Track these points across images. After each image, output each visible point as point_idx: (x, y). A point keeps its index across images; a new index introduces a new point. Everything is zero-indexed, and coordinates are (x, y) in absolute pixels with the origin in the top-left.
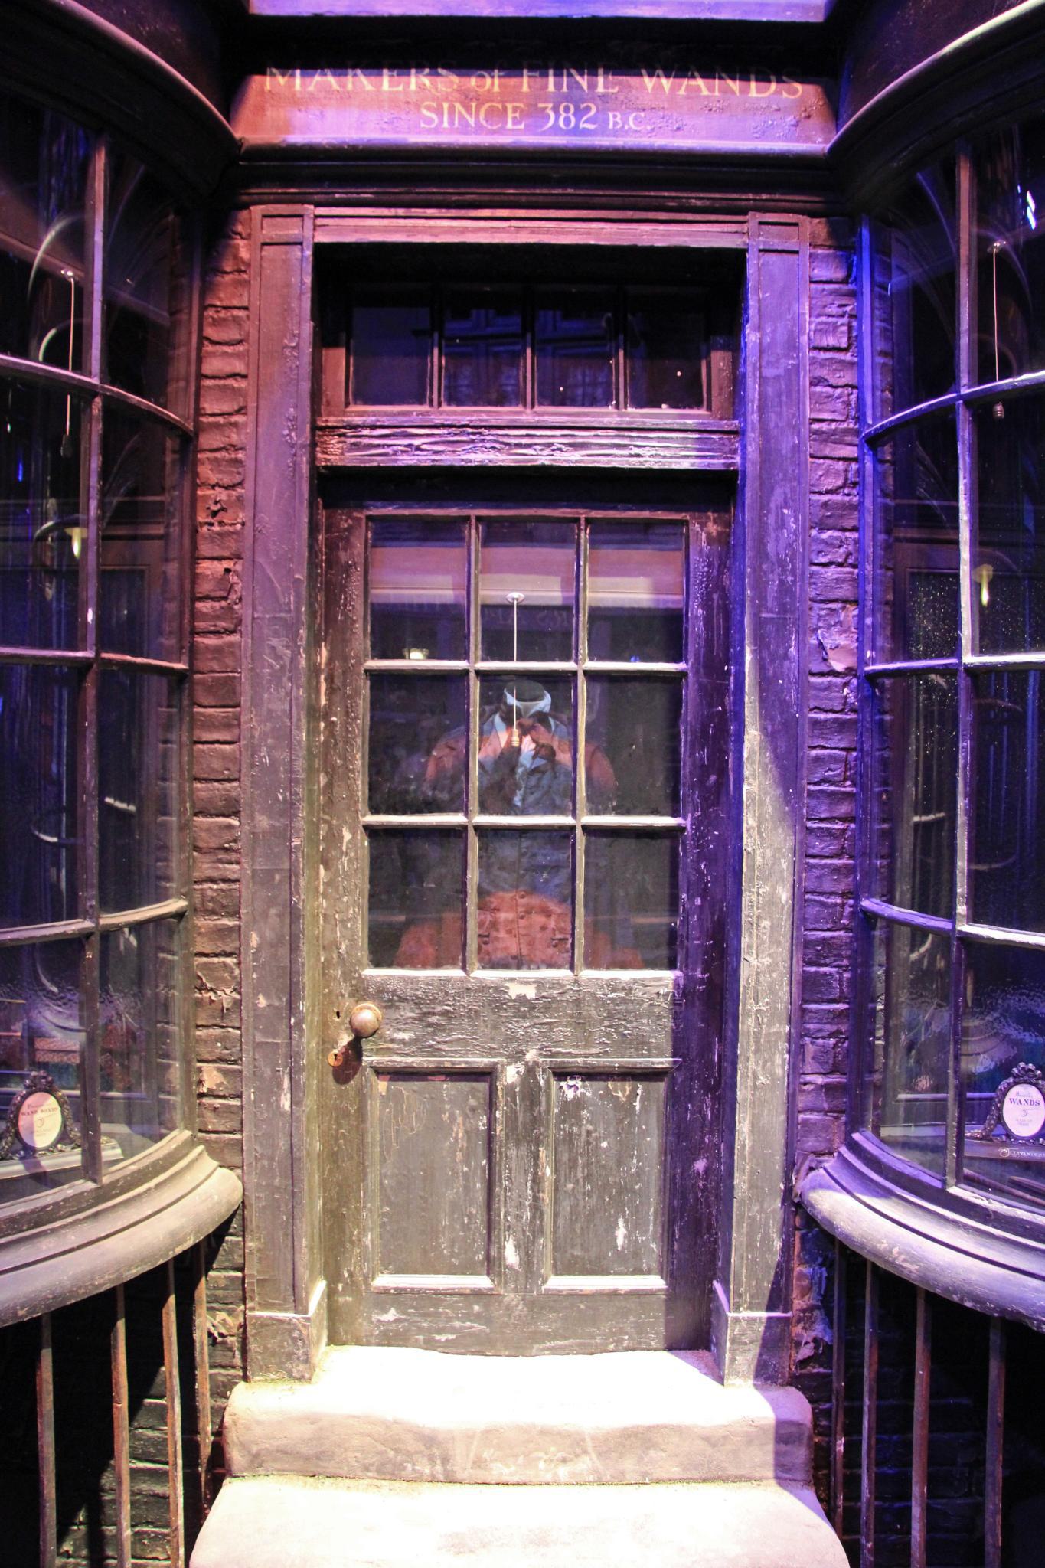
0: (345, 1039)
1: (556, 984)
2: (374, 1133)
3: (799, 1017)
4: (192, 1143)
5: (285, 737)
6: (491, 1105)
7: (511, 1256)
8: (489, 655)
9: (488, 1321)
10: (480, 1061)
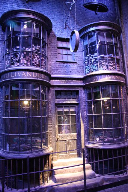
0: (57, 139)
3: (85, 135)
6: (66, 142)
10: (65, 140)
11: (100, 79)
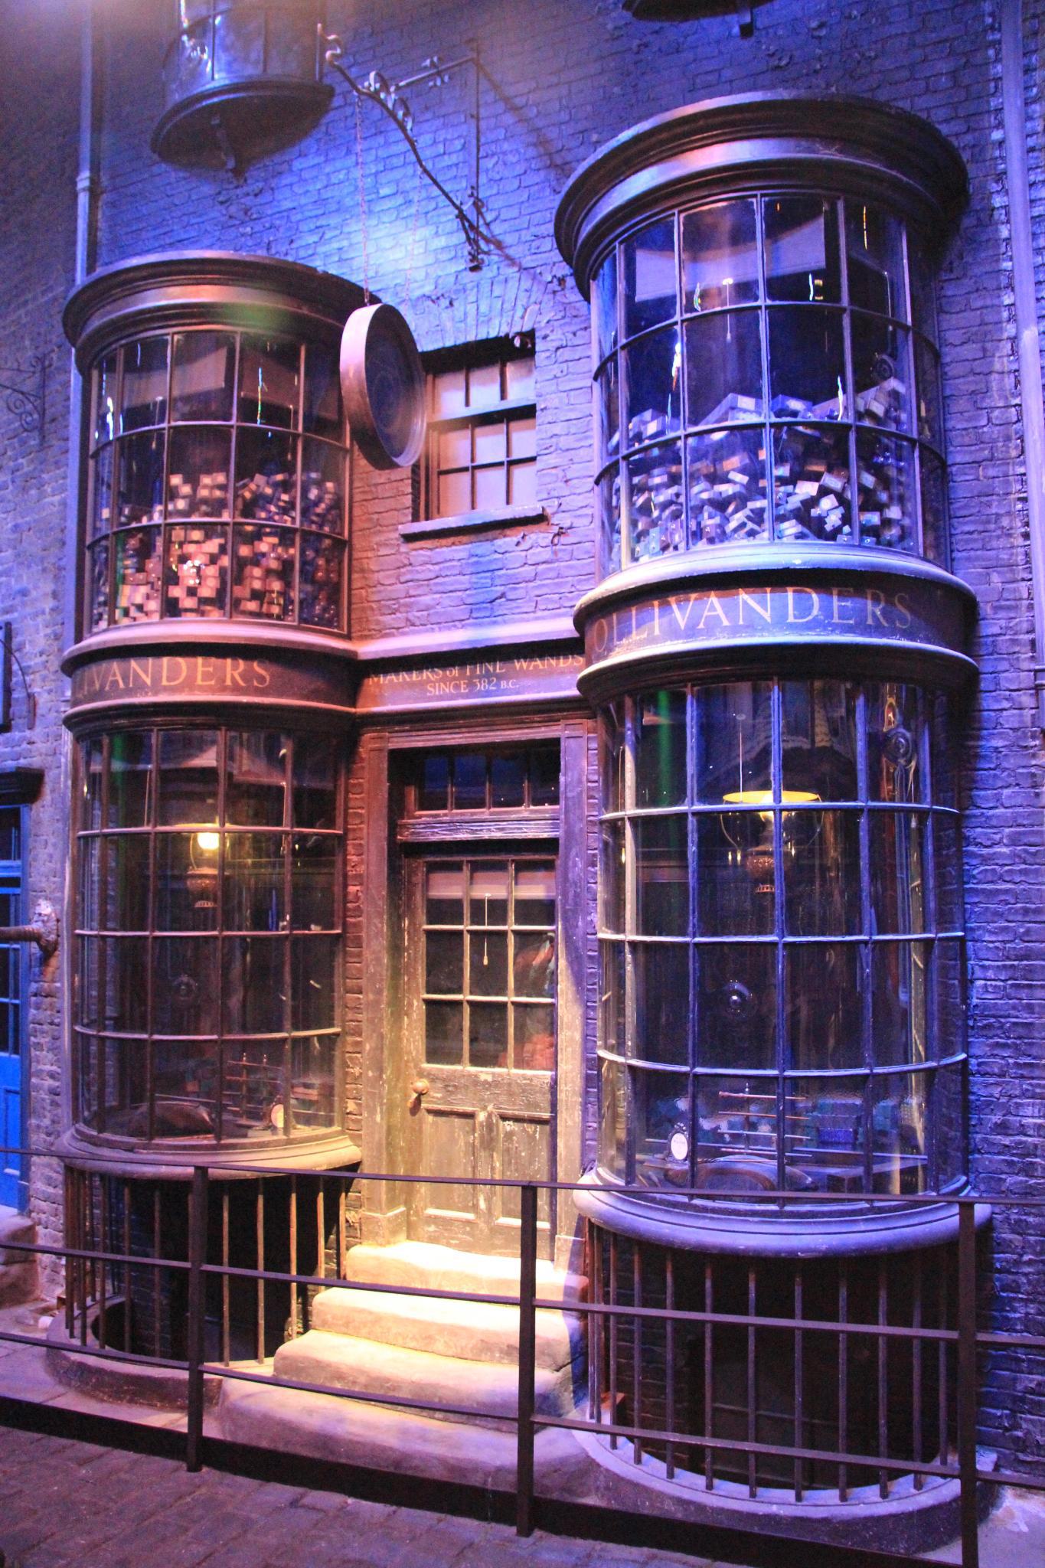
0: (415, 1095)
1: (500, 1075)
2: (426, 1141)
4: (342, 1133)
5: (378, 960)
7: (482, 1205)
8: (473, 923)
9: (473, 1236)
10: (469, 1109)
11: (620, 639)
